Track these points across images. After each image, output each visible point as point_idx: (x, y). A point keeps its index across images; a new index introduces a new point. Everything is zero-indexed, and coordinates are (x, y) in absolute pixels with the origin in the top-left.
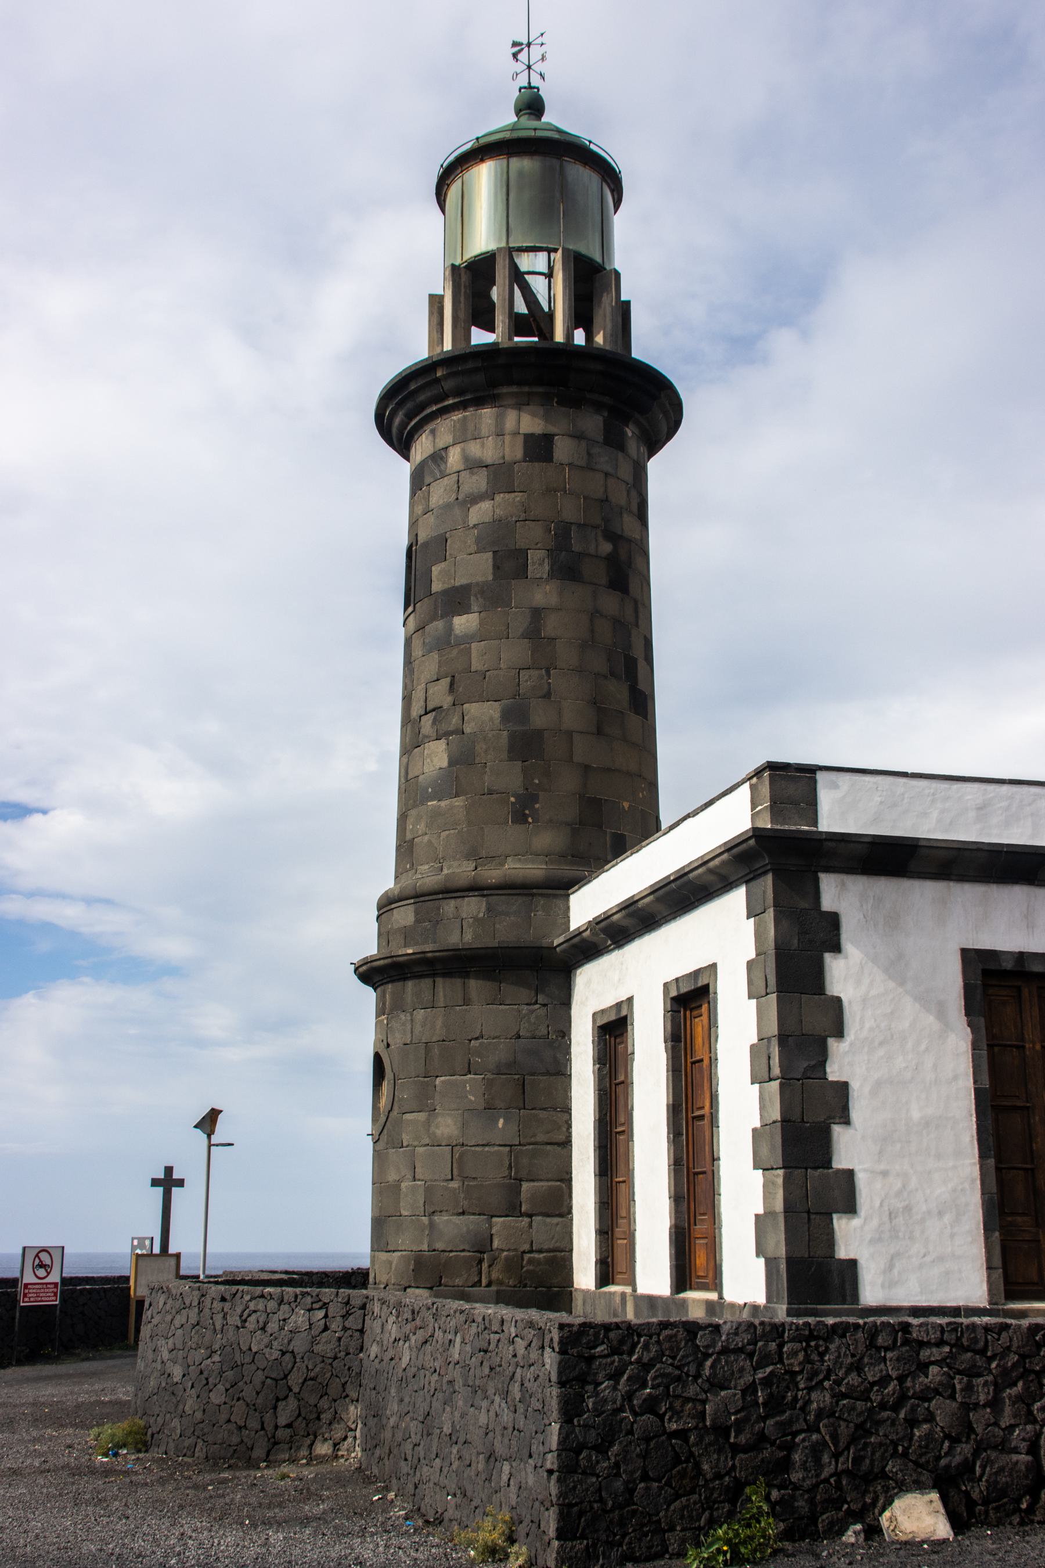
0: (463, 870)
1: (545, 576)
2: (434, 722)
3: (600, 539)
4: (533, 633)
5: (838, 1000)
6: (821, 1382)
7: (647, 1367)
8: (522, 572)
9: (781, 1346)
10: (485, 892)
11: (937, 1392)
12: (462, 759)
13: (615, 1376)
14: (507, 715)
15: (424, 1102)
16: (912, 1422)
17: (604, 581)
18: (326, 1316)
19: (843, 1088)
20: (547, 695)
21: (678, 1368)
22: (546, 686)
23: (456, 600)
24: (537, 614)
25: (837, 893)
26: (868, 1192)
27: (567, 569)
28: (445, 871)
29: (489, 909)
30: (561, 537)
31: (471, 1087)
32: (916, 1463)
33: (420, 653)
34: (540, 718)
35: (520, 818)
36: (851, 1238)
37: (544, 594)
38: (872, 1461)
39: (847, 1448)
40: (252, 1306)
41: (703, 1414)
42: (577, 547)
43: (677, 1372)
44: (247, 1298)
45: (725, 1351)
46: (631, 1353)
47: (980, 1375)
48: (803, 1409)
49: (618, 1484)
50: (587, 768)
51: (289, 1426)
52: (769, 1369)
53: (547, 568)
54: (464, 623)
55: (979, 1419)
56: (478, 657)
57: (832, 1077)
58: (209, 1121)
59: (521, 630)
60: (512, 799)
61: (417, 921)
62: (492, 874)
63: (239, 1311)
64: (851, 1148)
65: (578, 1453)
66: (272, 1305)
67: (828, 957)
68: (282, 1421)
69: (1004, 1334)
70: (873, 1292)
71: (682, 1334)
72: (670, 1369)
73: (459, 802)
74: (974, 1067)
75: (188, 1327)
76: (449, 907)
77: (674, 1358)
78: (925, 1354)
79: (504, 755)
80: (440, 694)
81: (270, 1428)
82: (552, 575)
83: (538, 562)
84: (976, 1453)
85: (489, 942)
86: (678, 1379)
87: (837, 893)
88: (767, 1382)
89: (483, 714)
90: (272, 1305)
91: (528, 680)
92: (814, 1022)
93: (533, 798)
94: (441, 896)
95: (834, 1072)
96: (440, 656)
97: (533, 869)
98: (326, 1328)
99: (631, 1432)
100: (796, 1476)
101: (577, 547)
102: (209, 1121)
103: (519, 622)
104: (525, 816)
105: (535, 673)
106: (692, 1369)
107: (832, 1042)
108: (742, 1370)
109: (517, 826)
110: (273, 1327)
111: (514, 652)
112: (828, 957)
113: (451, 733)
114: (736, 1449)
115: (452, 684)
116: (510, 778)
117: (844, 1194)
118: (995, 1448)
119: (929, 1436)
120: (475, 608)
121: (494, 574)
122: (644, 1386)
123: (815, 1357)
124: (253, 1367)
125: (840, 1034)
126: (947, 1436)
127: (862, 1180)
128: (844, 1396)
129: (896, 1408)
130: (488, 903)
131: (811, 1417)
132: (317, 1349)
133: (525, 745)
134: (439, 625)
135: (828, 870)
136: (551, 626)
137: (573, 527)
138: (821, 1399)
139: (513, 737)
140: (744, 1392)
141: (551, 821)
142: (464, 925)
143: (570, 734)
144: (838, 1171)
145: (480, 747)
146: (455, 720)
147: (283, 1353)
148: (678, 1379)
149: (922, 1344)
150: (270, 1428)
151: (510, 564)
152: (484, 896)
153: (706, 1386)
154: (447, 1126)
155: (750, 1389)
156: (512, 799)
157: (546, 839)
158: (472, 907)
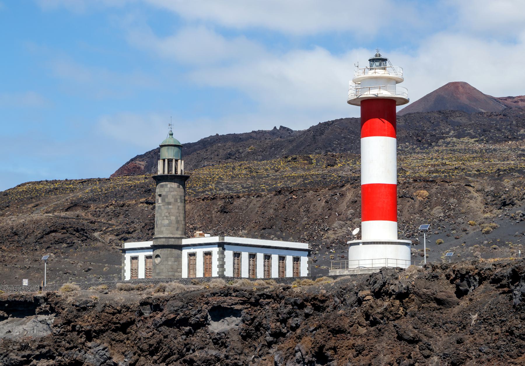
0: (172, 236)
4: (178, 209)
8: (177, 201)
15: (167, 260)
23: (169, 204)
24: (179, 206)
25: (225, 246)
26: (226, 270)
31: (173, 259)
34: (179, 219)
35: (177, 230)
37: (179, 204)
54: (170, 207)
56: (172, 211)
64: (225, 266)
76: (170, 239)
80: (167, 214)
87: (225, 246)
89: (173, 218)
97: (179, 236)
116: (176, 226)
133: (178, 222)
134: (167, 206)
136: (180, 208)
142: (172, 242)
151: (176, 200)
154: (170, 263)
157: (180, 232)
158: (173, 240)
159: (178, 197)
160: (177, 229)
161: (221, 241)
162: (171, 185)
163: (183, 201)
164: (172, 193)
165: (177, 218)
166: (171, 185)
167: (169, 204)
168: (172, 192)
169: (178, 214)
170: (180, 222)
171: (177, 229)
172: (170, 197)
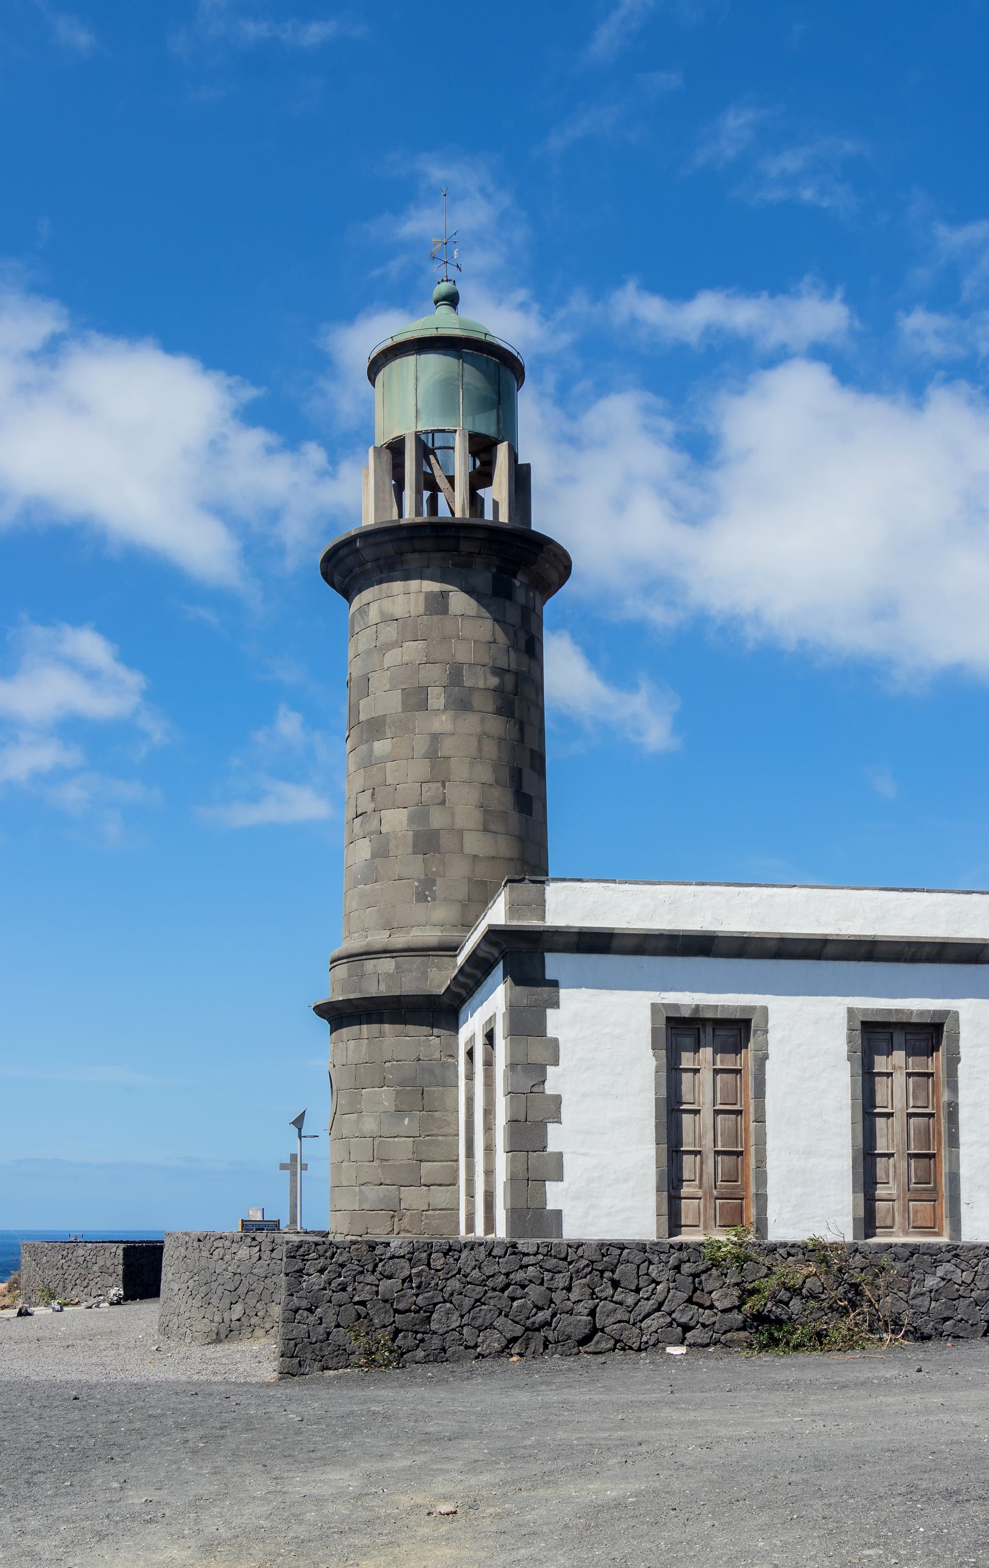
0: (380, 939)
1: (442, 708)
2: (361, 825)
3: (489, 675)
4: (432, 755)
5: (555, 1041)
6: (454, 1275)
7: (342, 1266)
9: (430, 1255)
10: (394, 954)
11: (531, 1281)
12: (381, 852)
13: (321, 1271)
14: (412, 819)
16: (513, 1299)
17: (490, 707)
18: (260, 1250)
19: (557, 1100)
20: (443, 803)
21: (362, 1266)
22: (442, 795)
24: (435, 738)
25: (555, 965)
27: (461, 703)
28: (369, 938)
29: (397, 967)
30: (455, 675)
31: (386, 1097)
32: (512, 1320)
33: (354, 769)
34: (437, 820)
35: (422, 897)
36: (556, 1196)
37: (442, 722)
38: (484, 1320)
39: (469, 1312)
40: (216, 1244)
41: (377, 1293)
42: (468, 683)
43: (361, 1269)
44: (212, 1239)
45: (392, 1257)
46: (332, 1258)
47: (560, 1272)
48: (441, 1290)
49: (321, 1329)
50: (475, 856)
51: (239, 1320)
52: (420, 1268)
53: (442, 701)
54: (381, 747)
55: (558, 1297)
56: (392, 772)
57: (548, 1092)
58: (299, 1122)
59: (423, 751)
60: (416, 884)
61: (350, 976)
62: (400, 940)
63: (208, 1246)
65: (296, 1311)
66: (228, 1243)
67: (549, 1011)
68: (235, 1317)
69: (581, 1249)
70: (572, 1231)
71: (365, 1248)
72: (356, 1267)
73: (377, 886)
74: (656, 1084)
75: (181, 1258)
76: (370, 965)
77: (359, 1261)
78: (526, 1260)
79: (410, 850)
81: (227, 1321)
82: (446, 708)
83: (437, 699)
84: (554, 1315)
85: (397, 992)
86: (362, 1272)
87: (555, 965)
88: (419, 1274)
90: (228, 1243)
91: (431, 790)
92: (537, 1053)
93: (433, 882)
94: (364, 957)
95: (550, 1088)
96: (365, 772)
98: (260, 1259)
99: (330, 1301)
100: (434, 1326)
101: (468, 683)
102: (299, 1122)
103: (421, 745)
104: (427, 896)
105: (434, 786)
106: (370, 1267)
107: (550, 1069)
108: (402, 1268)
109: (420, 904)
110: (227, 1257)
111: (421, 768)
112: (549, 1011)
113: (373, 833)
114: (397, 1311)
115: (373, 795)
116: (415, 867)
117: (556, 1168)
118: (567, 1313)
119: (523, 1306)
120: (388, 735)
121: (403, 707)
122: (340, 1276)
123: (451, 1260)
124: (216, 1284)
125: (556, 1063)
126: (536, 1306)
127: (566, 1159)
128: (469, 1283)
129: (503, 1290)
130: (396, 962)
131: (446, 1296)
132: (255, 1271)
133: (427, 842)
135: (550, 950)
136: (446, 748)
137: (465, 666)
138: (454, 1284)
139: (417, 835)
140: (404, 1281)
141: (445, 899)
142: (381, 979)
143: (461, 832)
144: (551, 1153)
145: (392, 844)
146: (375, 823)
147: (235, 1274)
148: (362, 1272)
149: (525, 1255)
150: (227, 1321)
151: (416, 699)
152: (393, 957)
153: (380, 1276)
155: (409, 1278)
156: (416, 884)
158: (387, 965)
159: (435, 674)
160: (424, 893)
161: (515, 923)
162: (387, 605)
163: (485, 703)
164: (393, 657)
165: (420, 814)
166: (387, 605)
167: (375, 728)
168: (389, 646)
169: (431, 790)
170: (446, 841)
171: (424, 893)
172: (380, 682)
